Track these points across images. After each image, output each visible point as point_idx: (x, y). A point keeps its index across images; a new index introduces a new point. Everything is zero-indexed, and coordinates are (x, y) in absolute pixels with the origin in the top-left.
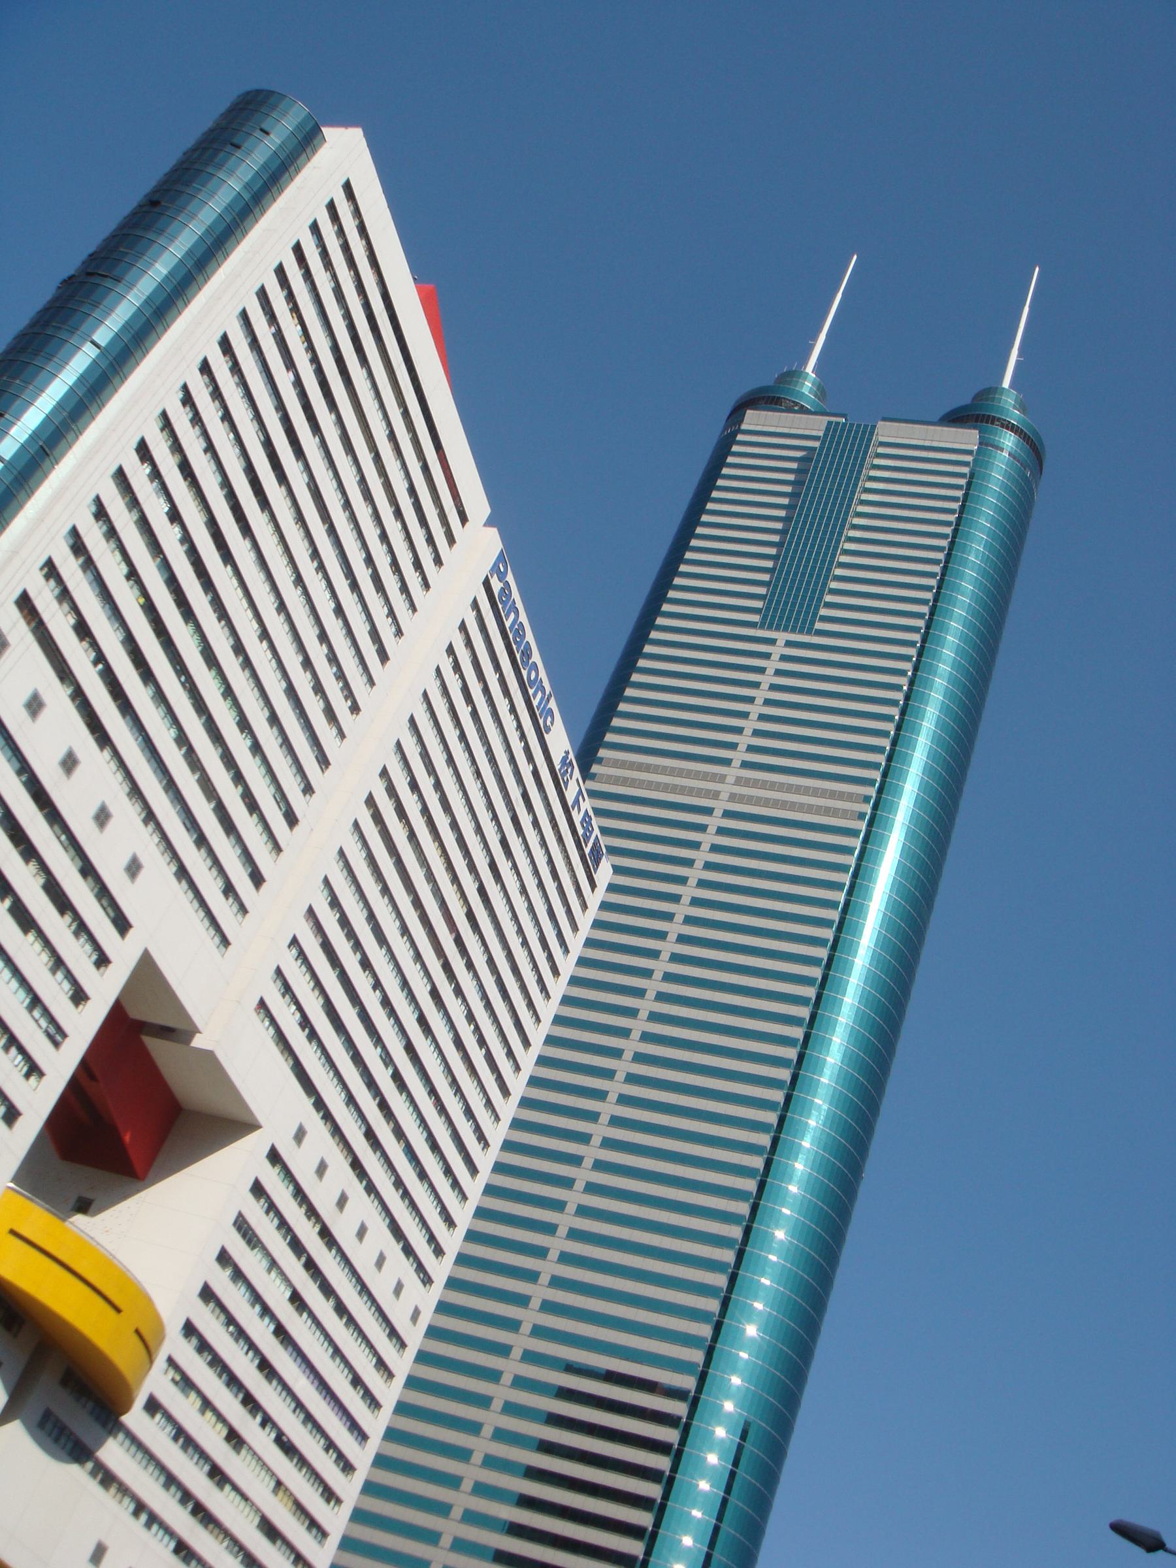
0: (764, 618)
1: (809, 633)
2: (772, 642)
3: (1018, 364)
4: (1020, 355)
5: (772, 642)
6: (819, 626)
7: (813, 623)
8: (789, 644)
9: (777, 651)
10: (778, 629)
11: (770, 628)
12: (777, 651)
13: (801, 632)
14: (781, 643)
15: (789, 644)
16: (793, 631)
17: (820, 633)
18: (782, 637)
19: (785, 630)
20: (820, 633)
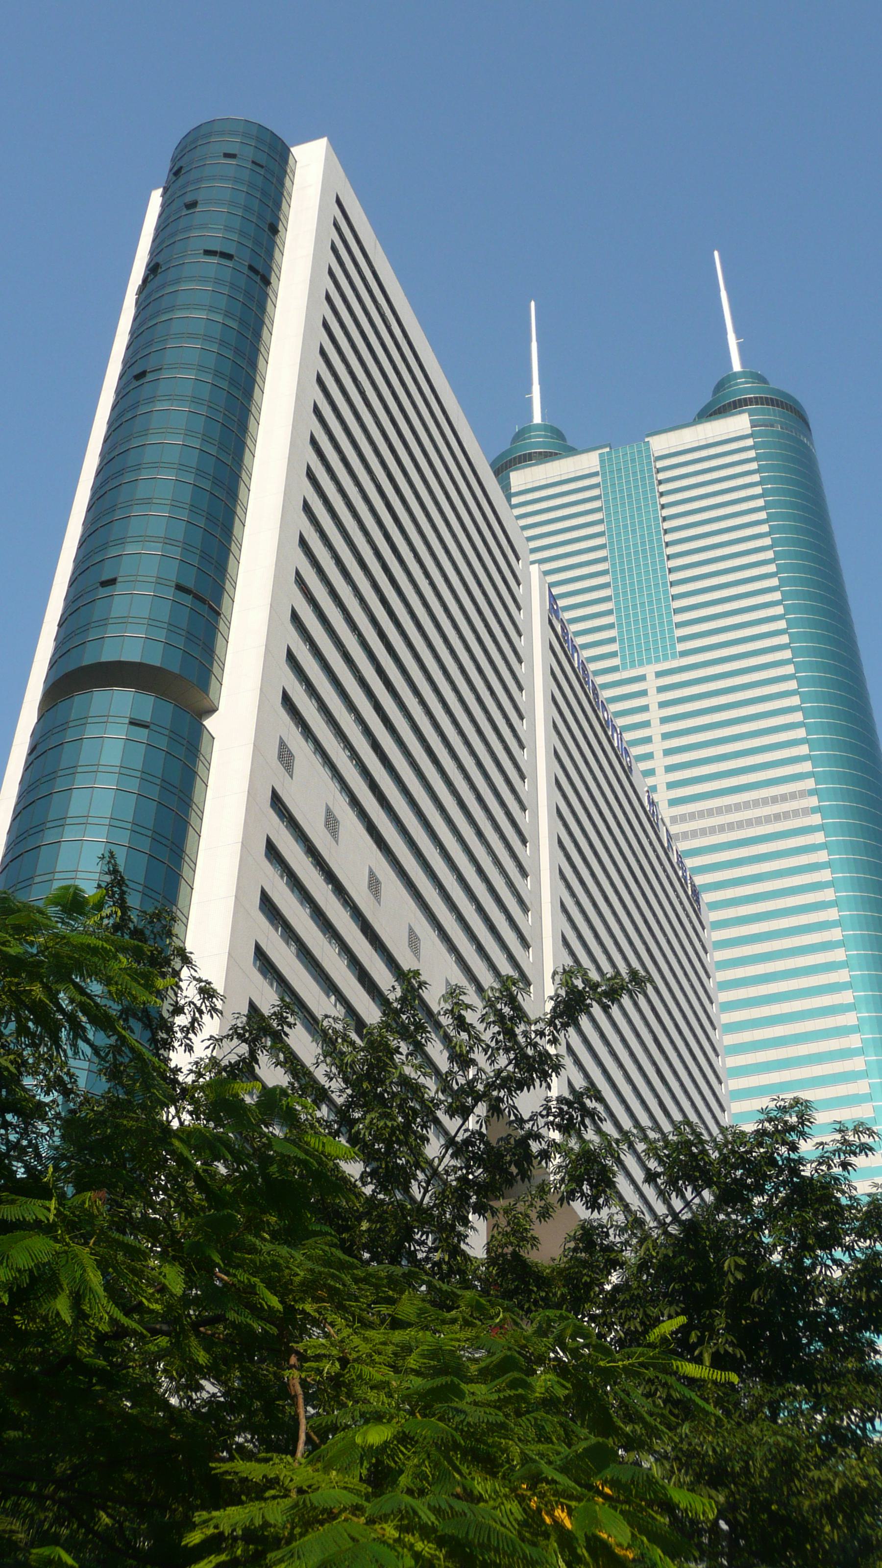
0: (623, 658)
1: (674, 656)
2: (642, 678)
3: (739, 345)
4: (738, 338)
5: (642, 678)
6: (680, 647)
7: (673, 646)
8: (659, 674)
9: (652, 684)
10: (641, 664)
11: (633, 666)
12: (652, 684)
13: (666, 658)
14: (651, 676)
15: (659, 674)
16: (657, 660)
17: (684, 654)
18: (649, 670)
19: (649, 662)
20: (684, 654)
